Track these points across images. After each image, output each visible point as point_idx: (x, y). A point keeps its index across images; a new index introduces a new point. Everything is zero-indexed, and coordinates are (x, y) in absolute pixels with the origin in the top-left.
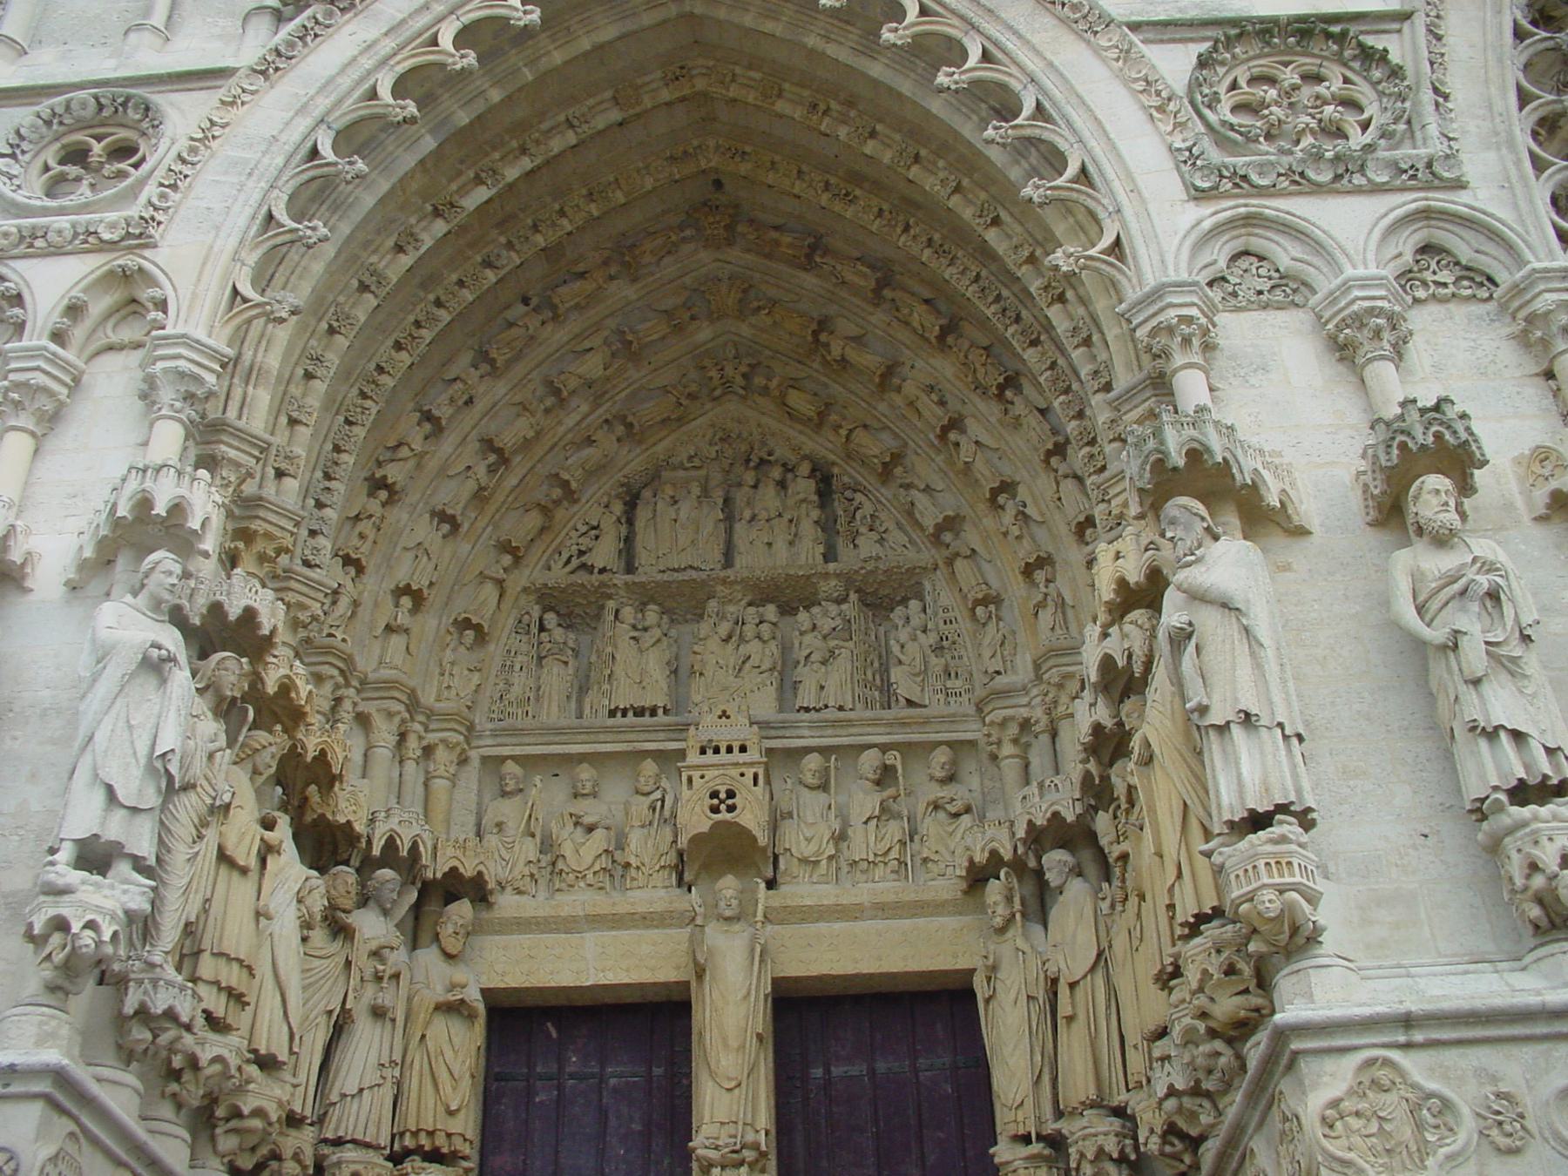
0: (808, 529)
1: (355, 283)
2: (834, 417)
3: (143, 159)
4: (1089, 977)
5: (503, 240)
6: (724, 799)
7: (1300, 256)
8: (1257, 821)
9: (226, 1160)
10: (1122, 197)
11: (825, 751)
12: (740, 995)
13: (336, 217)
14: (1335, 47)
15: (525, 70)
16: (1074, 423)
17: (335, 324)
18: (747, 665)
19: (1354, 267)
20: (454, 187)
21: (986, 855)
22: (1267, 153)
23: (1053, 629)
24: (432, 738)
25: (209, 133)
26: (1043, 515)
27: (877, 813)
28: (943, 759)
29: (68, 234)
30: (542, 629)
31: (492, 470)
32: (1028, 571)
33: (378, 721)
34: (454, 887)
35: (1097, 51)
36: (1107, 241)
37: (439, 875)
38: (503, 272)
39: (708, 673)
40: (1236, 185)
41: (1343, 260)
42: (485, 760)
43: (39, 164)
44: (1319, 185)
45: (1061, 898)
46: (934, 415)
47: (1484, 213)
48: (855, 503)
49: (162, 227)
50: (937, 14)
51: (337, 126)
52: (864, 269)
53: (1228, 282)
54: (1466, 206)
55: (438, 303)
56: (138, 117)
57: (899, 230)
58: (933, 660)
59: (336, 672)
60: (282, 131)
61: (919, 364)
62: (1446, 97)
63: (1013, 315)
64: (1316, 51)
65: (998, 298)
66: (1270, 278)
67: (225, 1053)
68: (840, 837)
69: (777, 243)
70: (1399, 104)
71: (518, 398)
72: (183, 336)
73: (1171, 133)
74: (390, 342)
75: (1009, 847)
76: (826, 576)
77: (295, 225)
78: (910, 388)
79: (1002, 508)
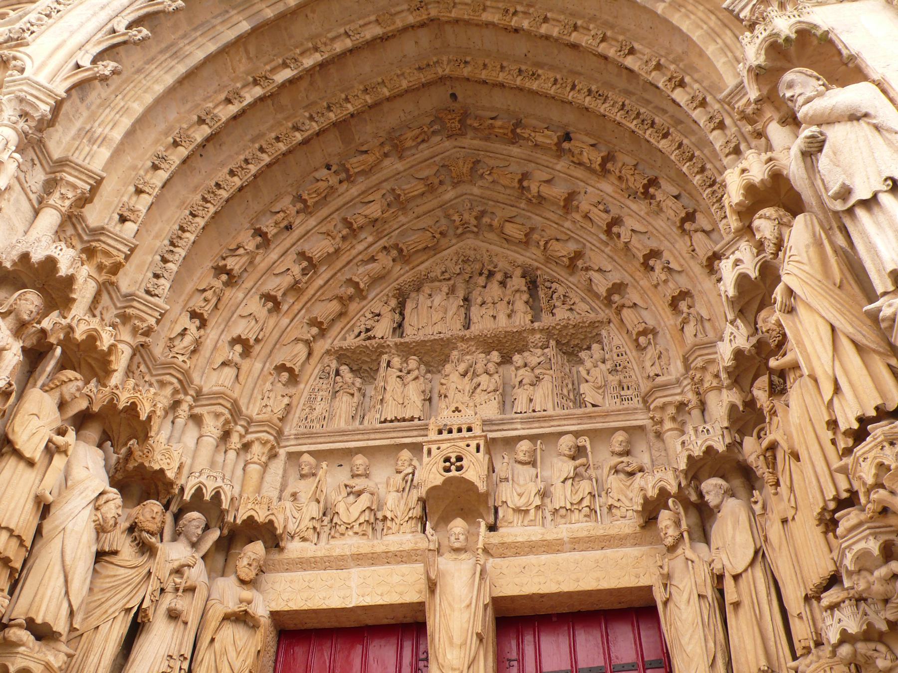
0: (520, 305)
2: (535, 236)
4: (750, 570)
5: (307, 114)
6: (454, 462)
11: (533, 438)
12: (464, 604)
17: (178, 140)
18: (478, 390)
20: (268, 68)
21: (657, 491)
23: (695, 335)
24: (250, 437)
26: (682, 266)
27: (572, 475)
28: (621, 438)
30: (337, 373)
31: (304, 272)
32: (674, 304)
37: (239, 521)
38: (306, 134)
39: (451, 394)
42: (290, 455)
45: (719, 515)
46: (602, 219)
52: (549, 133)
55: (262, 150)
57: (568, 89)
58: (611, 377)
59: (175, 381)
61: (590, 189)
63: (650, 122)
65: (638, 114)
68: (544, 494)
69: (492, 127)
71: (324, 230)
74: (226, 170)
76: (533, 331)
78: (584, 206)
79: (652, 269)
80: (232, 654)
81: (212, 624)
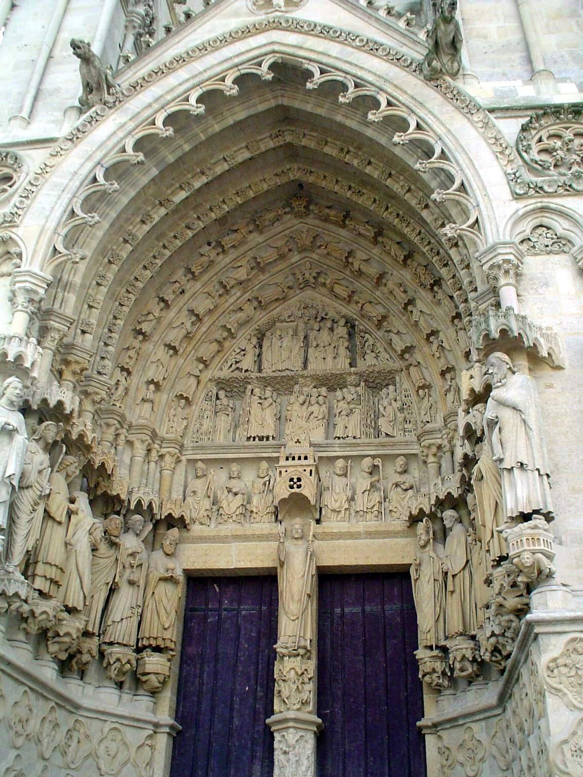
0: (342, 351)
1: (121, 239)
2: (356, 298)
5: (195, 216)
6: (295, 482)
7: (567, 227)
8: (525, 517)
9: (53, 656)
10: (480, 199)
11: (346, 458)
12: (300, 576)
13: (109, 208)
15: (201, 135)
16: (463, 305)
17: (111, 259)
18: (312, 416)
20: (169, 192)
21: (418, 511)
22: (553, 175)
24: (163, 451)
26: (451, 347)
27: (368, 488)
30: (218, 398)
31: (193, 324)
32: (443, 374)
33: (138, 444)
34: (171, 522)
35: (472, 122)
37: (163, 517)
38: (195, 232)
39: (294, 419)
40: (537, 192)
42: (189, 460)
45: (451, 533)
48: (365, 339)
50: (395, 105)
52: (369, 227)
53: (530, 240)
55: (164, 247)
56: (12, 162)
57: (383, 210)
58: (399, 415)
59: (116, 422)
60: (79, 169)
61: (395, 273)
63: (436, 251)
65: (429, 243)
66: (552, 239)
67: (47, 609)
68: (352, 499)
69: (328, 215)
71: (205, 290)
73: (506, 166)
74: (141, 266)
75: (428, 508)
76: (350, 374)
78: (390, 285)
79: (432, 343)
80: (164, 599)
81: (152, 583)
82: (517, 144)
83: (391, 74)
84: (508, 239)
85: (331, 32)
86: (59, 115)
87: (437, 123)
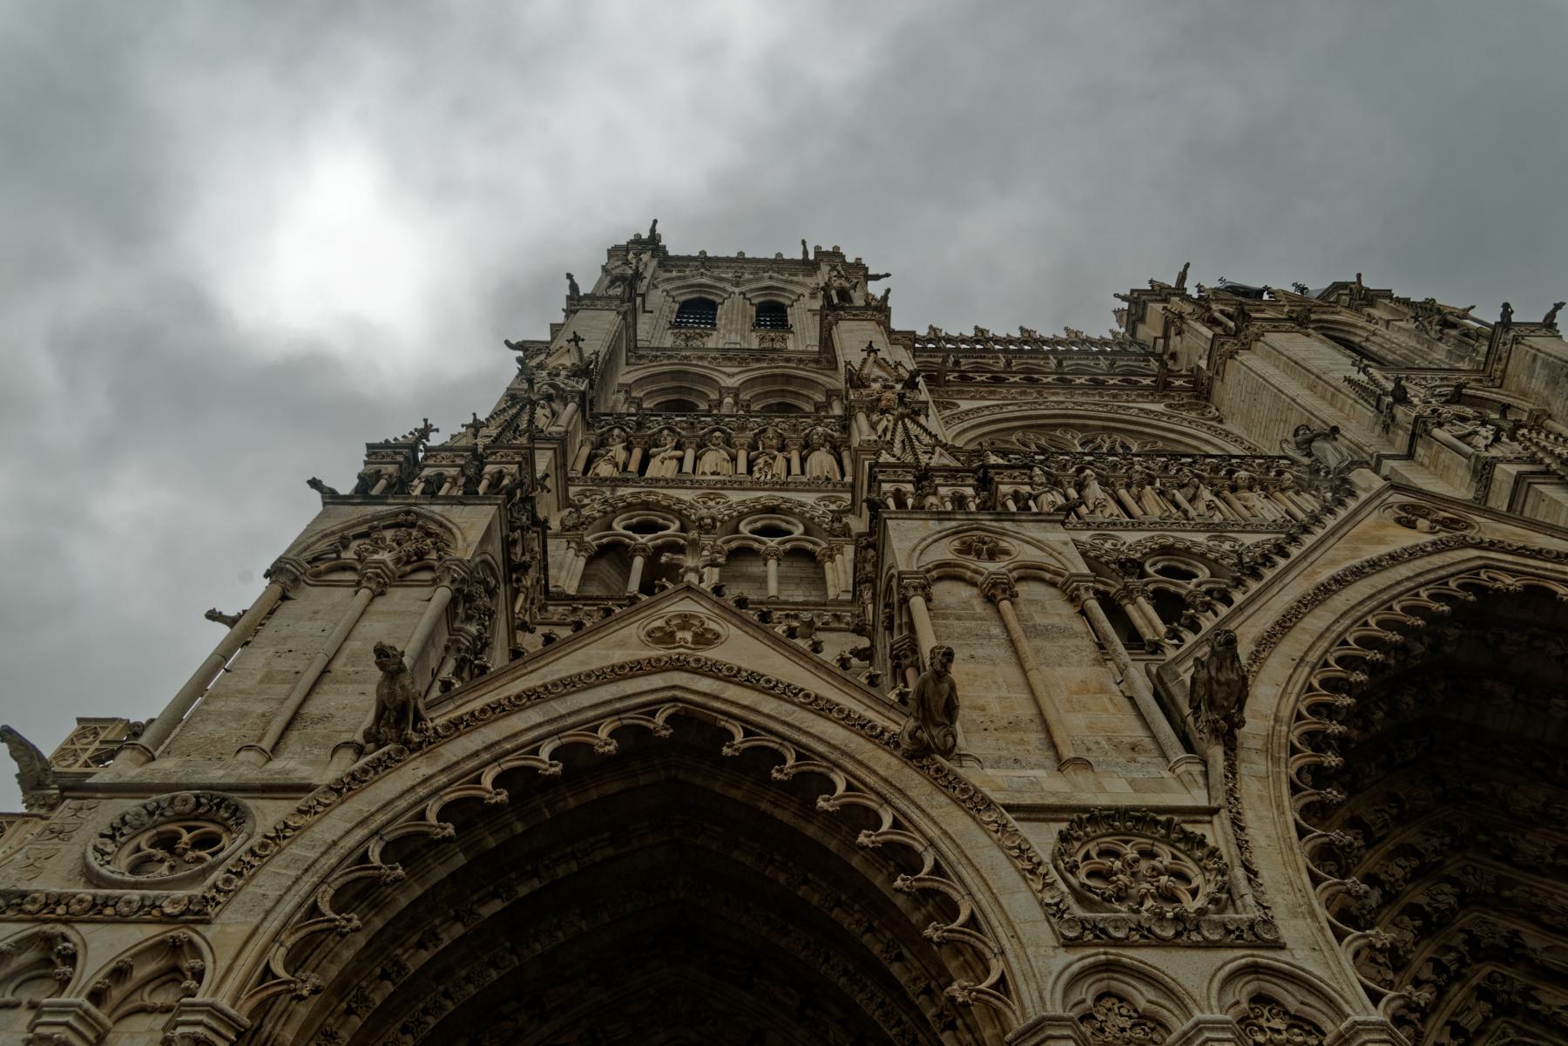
3: (222, 849)
7: (1153, 998)
13: (373, 912)
14: (1163, 831)
15: (546, 810)
17: (354, 1005)
19: (1202, 1011)
20: (475, 897)
25: (282, 834)
29: (135, 906)
35: (981, 824)
36: (994, 978)
38: (503, 972)
40: (1096, 937)
41: (1191, 1005)
43: (132, 845)
44: (1163, 939)
47: (1303, 970)
49: (220, 907)
51: (387, 838)
53: (1096, 1019)
54: (1286, 963)
55: (447, 995)
56: (226, 815)
57: (820, 960)
60: (342, 838)
62: (1256, 874)
64: (1149, 833)
65: (899, 1023)
66: (1130, 1017)
70: (1219, 878)
72: (212, 1006)
73: (1041, 891)
74: (398, 1026)
77: (333, 916)
82: (1054, 860)
83: (853, 746)
84: (1059, 1012)
85: (762, 682)
86: (324, 753)
87: (926, 820)
